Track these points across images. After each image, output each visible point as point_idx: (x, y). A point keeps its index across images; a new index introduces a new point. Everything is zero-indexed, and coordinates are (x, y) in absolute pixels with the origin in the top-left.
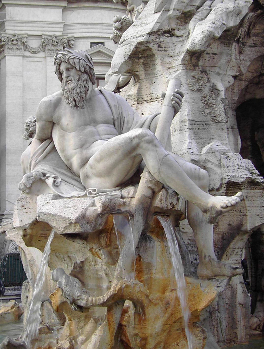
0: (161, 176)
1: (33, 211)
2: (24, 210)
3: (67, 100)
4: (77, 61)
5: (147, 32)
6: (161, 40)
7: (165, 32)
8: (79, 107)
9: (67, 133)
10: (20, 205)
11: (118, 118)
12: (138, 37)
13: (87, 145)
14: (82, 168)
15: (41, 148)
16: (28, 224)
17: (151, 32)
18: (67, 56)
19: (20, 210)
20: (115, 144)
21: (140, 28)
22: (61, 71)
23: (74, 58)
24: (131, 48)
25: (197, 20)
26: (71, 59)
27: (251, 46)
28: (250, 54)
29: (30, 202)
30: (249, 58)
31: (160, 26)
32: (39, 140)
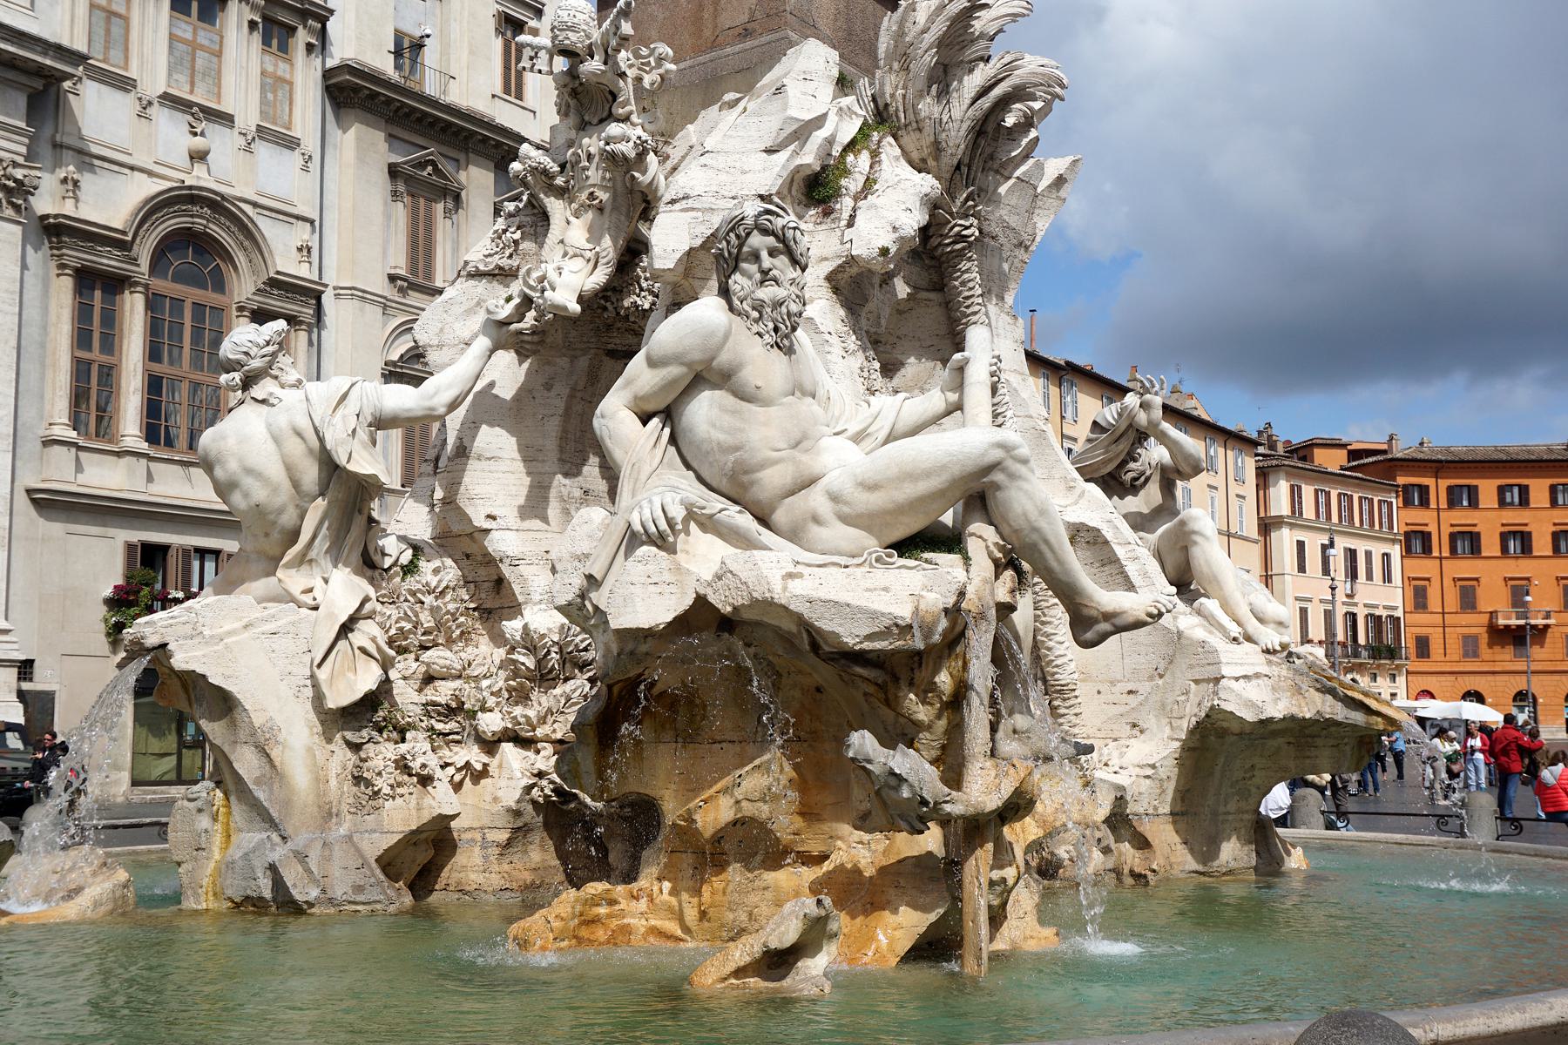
13: (805, 444)
21: (723, 177)
22: (745, 249)
23: (795, 228)
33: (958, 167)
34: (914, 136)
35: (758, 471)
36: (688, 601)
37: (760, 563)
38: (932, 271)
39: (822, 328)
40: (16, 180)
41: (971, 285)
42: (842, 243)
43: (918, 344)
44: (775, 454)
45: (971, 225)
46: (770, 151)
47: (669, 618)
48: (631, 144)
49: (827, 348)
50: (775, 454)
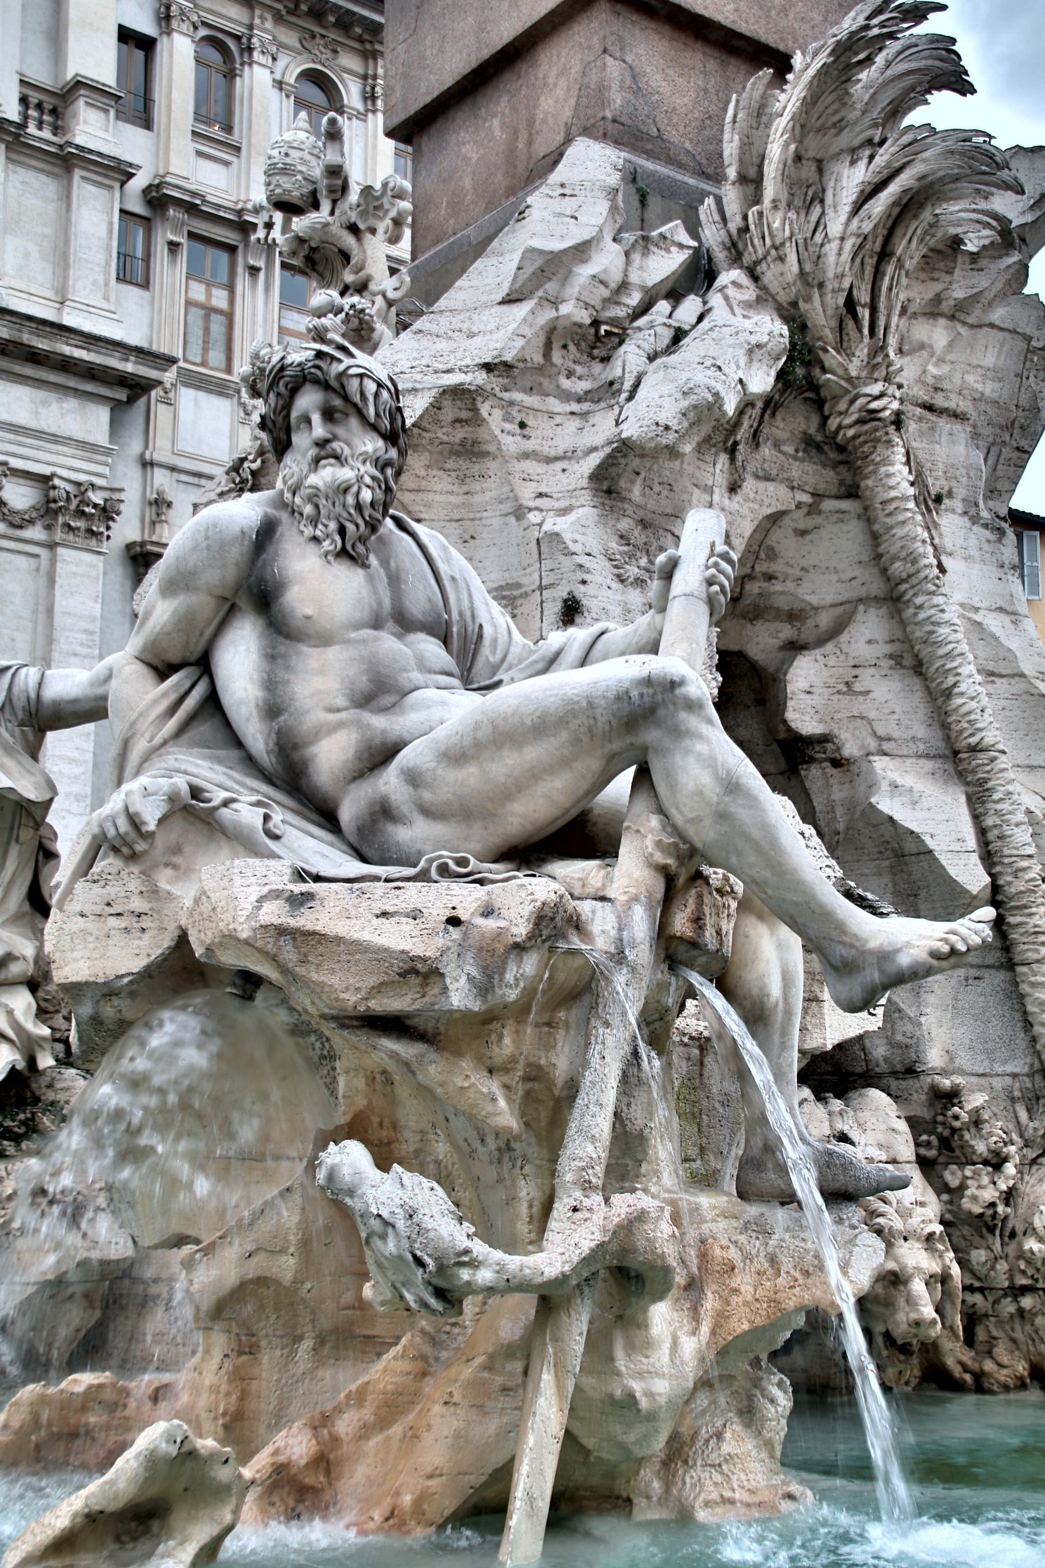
3: (311, 529)
4: (371, 387)
5: (478, 361)
9: (304, 648)
10: (98, 899)
14: (357, 783)
15: (165, 694)
16: (129, 974)
17: (496, 361)
18: (335, 365)
21: (442, 345)
23: (361, 376)
24: (416, 406)
25: (641, 353)
26: (352, 376)
27: (757, 477)
31: (523, 348)
32: (149, 665)
33: (850, 304)
34: (776, 268)
35: (312, 743)
36: (167, 941)
37: (237, 879)
38: (842, 469)
39: (573, 547)
40: (95, 506)
41: (892, 482)
42: (617, 424)
43: (834, 578)
44: (332, 717)
45: (882, 395)
46: (509, 300)
47: (137, 965)
48: (342, 315)
49: (580, 576)
50: (332, 717)
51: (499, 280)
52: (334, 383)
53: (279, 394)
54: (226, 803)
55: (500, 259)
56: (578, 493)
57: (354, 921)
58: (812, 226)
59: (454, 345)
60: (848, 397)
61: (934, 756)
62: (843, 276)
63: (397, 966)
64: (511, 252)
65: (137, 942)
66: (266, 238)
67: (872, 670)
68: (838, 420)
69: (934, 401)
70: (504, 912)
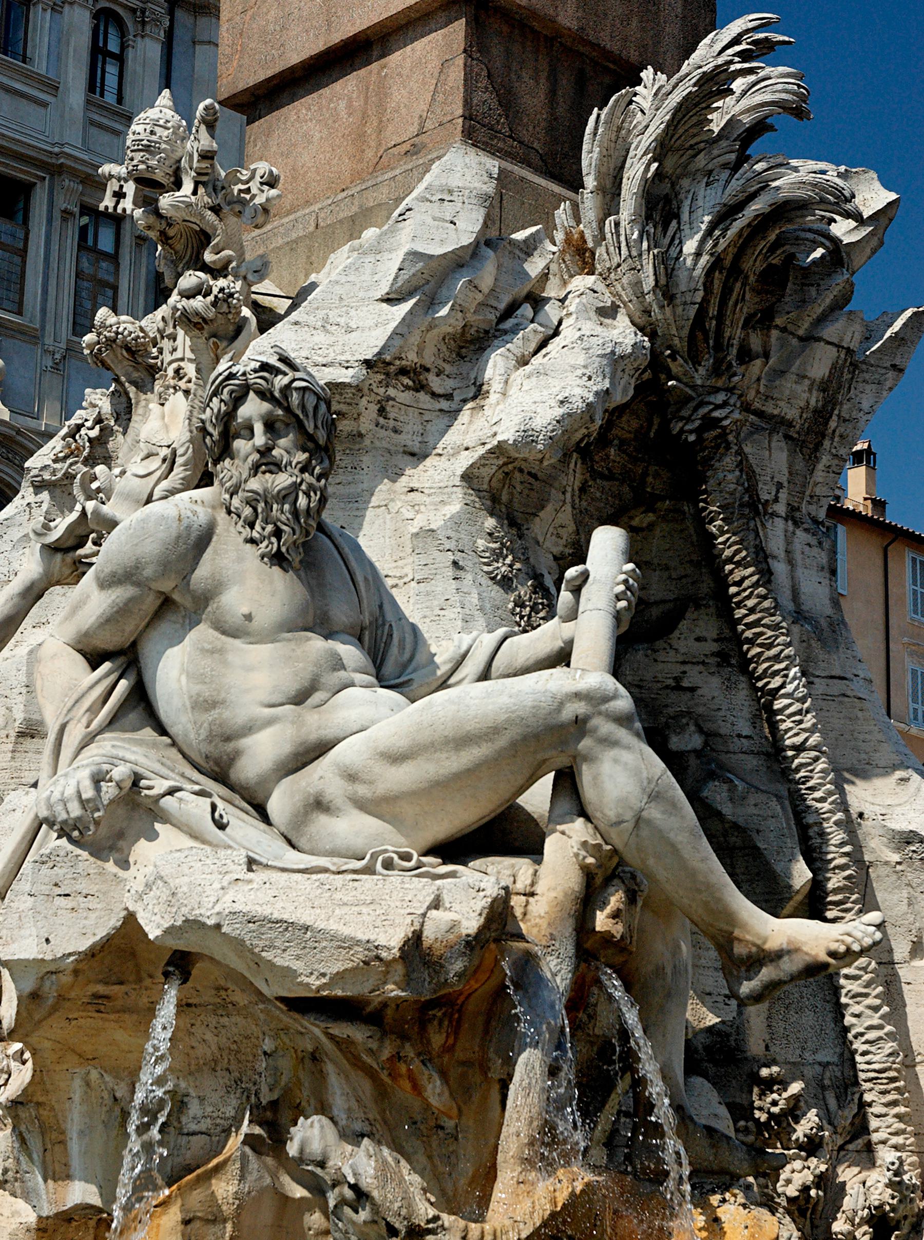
0: (637, 835)
1: (99, 906)
2: (62, 898)
6: (392, 392)
7: (403, 371)
8: (287, 559)
11: (370, 623)
12: (324, 365)
18: (280, 377)
19: (45, 898)
20: (490, 707)
21: (320, 338)
23: (304, 389)
25: (510, 355)
28: (600, 500)
29: (91, 871)
30: (598, 509)
36: (114, 921)
45: (725, 404)
46: (388, 300)
47: (84, 945)
48: (211, 298)
51: (376, 278)
52: (277, 394)
53: (222, 400)
54: (171, 792)
55: (378, 257)
56: (449, 490)
57: (318, 911)
58: (667, 241)
59: (333, 339)
60: (692, 405)
61: (758, 753)
62: (696, 290)
63: (360, 954)
64: (390, 251)
65: (85, 922)
66: (115, 208)
67: (700, 668)
68: (680, 424)
69: (764, 408)
70: (456, 907)
